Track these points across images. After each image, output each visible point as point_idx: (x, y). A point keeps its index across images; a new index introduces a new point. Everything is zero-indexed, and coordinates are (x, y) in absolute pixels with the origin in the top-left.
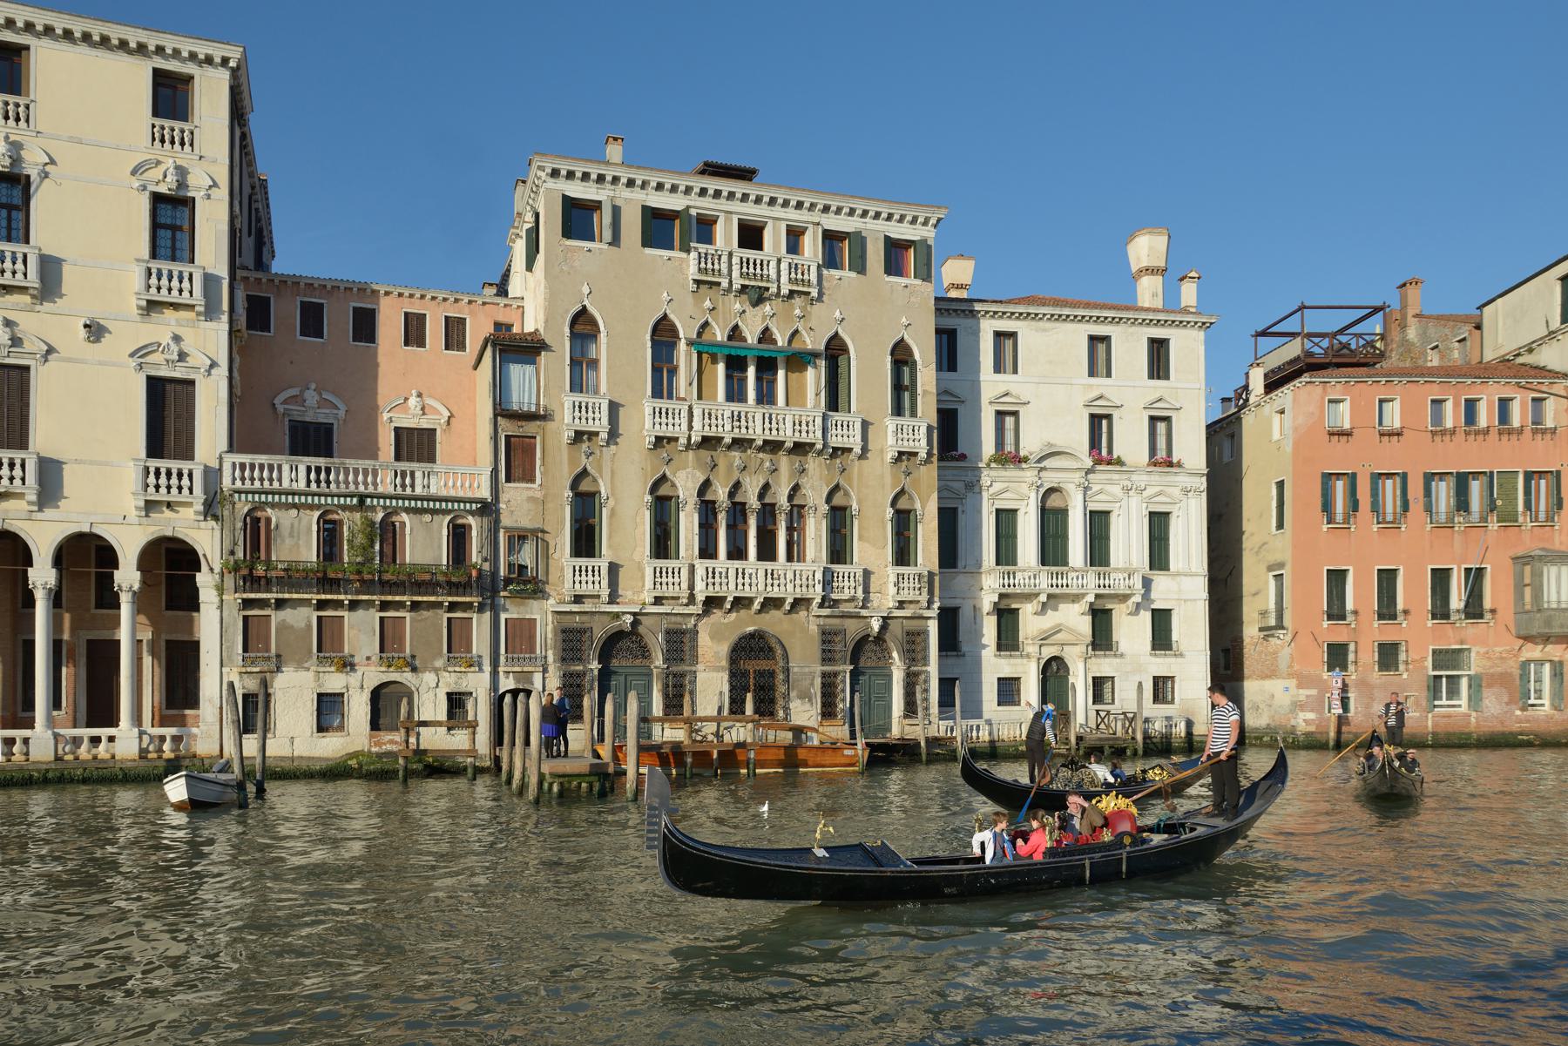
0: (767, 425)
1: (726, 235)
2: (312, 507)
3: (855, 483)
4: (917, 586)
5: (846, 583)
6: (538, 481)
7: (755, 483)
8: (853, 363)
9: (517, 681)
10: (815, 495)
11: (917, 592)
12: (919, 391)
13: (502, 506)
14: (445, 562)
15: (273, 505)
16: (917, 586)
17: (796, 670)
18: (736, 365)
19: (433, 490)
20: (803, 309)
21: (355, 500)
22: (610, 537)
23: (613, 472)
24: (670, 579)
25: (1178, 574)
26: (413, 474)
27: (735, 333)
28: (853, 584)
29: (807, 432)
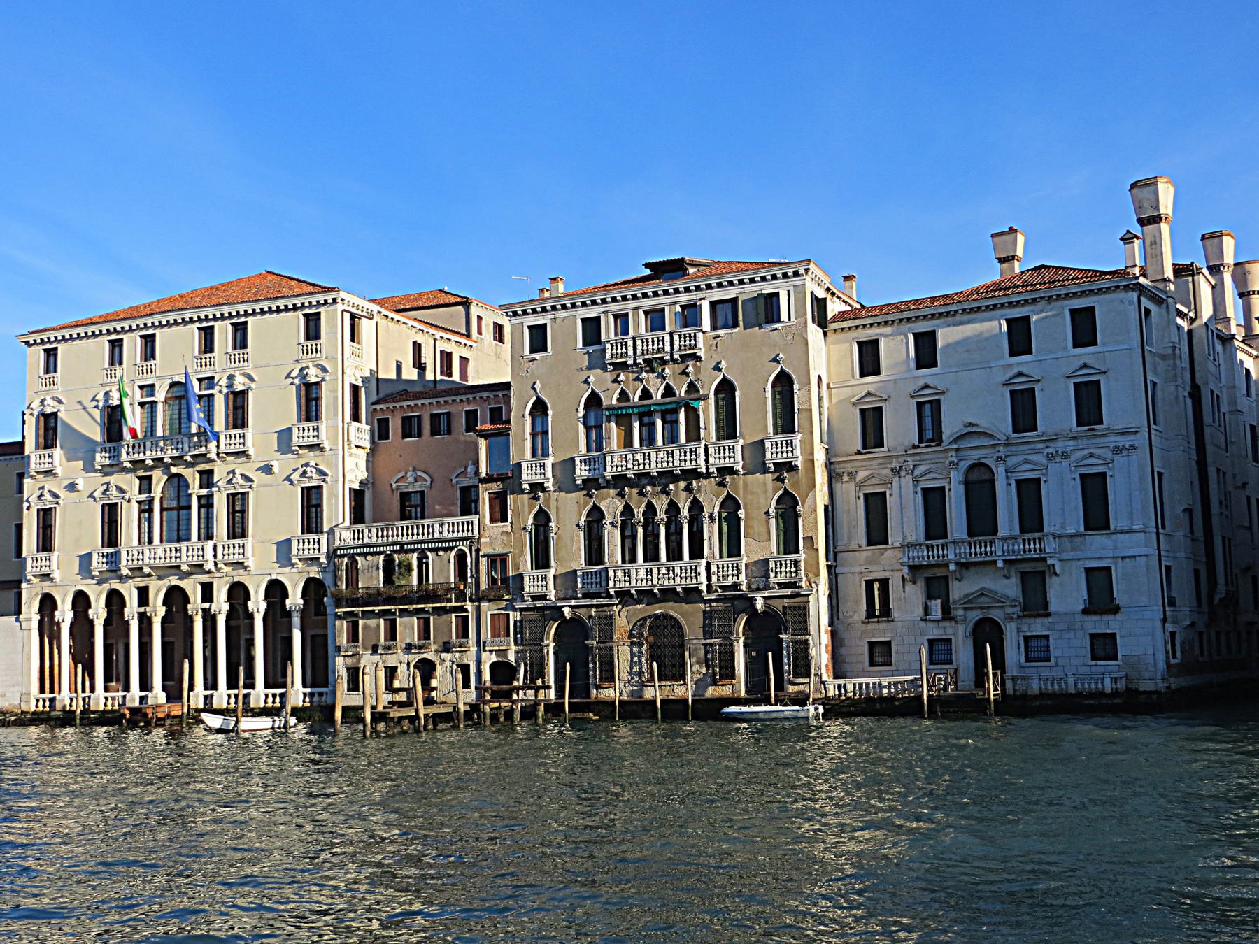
0: (683, 458)
1: (639, 325)
2: (379, 553)
3: (741, 492)
4: (793, 569)
5: (730, 572)
6: (510, 520)
7: (659, 502)
8: (737, 399)
9: (497, 656)
10: (712, 506)
11: (793, 575)
12: (796, 410)
13: (482, 540)
14: (452, 580)
15: (359, 555)
16: (793, 569)
17: (695, 641)
18: (645, 416)
19: (445, 534)
20: (694, 366)
21: (398, 547)
22: (557, 553)
23: (557, 508)
24: (594, 580)
25: (1117, 532)
26: (433, 525)
27: (646, 394)
28: (735, 572)
29: (691, 460)
